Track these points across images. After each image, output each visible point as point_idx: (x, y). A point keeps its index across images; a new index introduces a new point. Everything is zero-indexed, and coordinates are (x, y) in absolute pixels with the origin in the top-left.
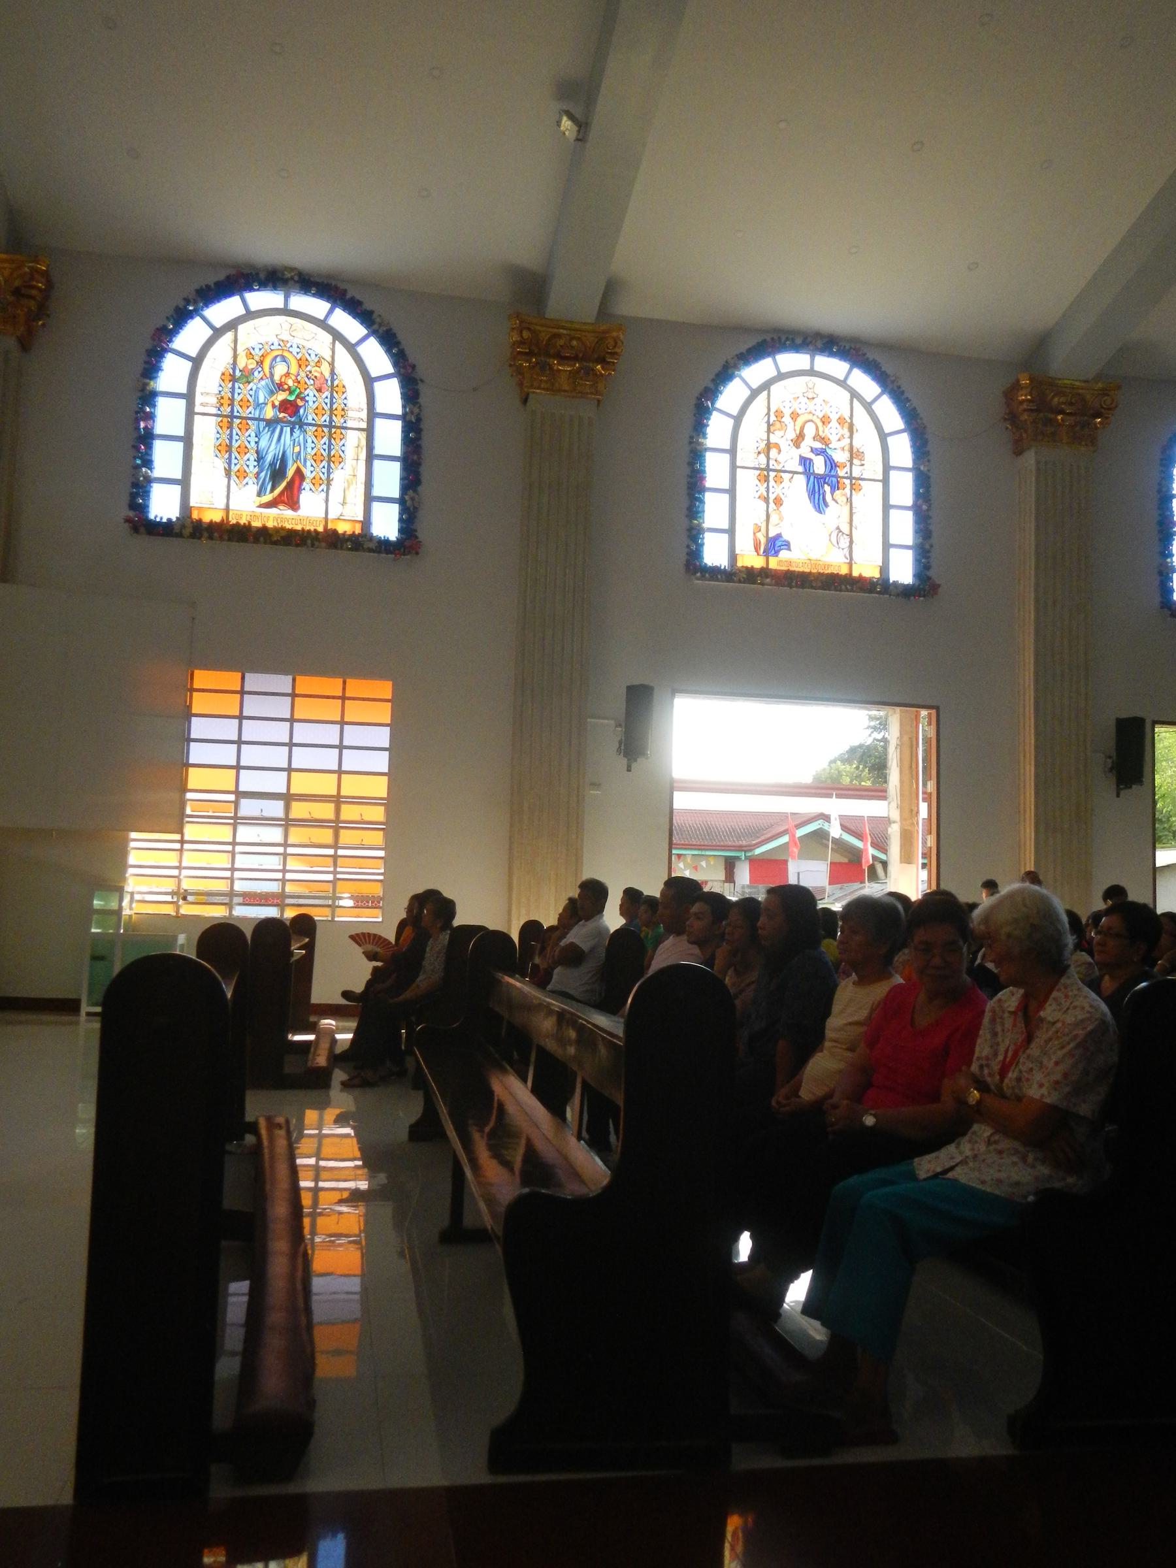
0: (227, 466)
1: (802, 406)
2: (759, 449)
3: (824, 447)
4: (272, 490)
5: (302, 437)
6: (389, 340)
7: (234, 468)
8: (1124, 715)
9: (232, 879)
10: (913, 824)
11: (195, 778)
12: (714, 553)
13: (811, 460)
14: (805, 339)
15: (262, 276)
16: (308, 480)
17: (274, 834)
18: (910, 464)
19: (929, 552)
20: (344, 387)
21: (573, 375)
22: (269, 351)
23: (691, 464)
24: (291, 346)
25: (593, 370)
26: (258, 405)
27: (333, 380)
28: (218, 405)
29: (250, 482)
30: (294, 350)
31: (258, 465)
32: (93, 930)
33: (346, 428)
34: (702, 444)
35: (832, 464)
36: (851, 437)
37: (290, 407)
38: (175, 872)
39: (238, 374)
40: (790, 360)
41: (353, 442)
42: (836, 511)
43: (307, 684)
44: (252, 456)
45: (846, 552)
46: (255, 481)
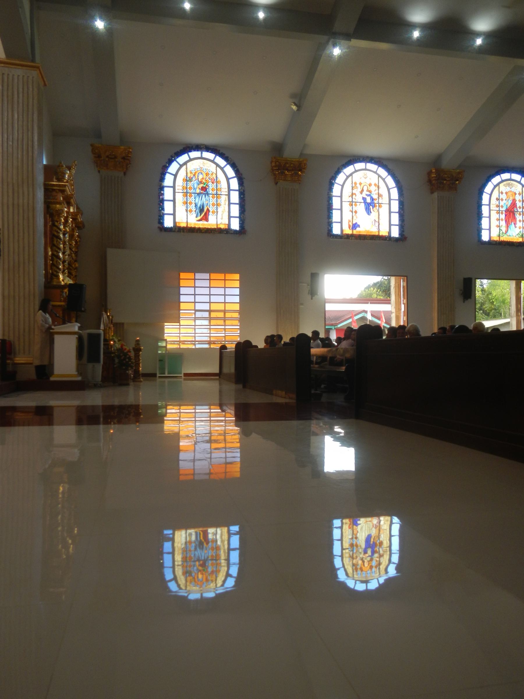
0: (186, 209)
1: (363, 181)
2: (350, 195)
3: (370, 193)
4: (200, 216)
5: (208, 198)
6: (234, 166)
7: (189, 209)
8: (466, 276)
9: (195, 337)
10: (400, 313)
11: (182, 306)
12: (336, 230)
13: (366, 198)
14: (363, 158)
15: (194, 147)
17: (206, 322)
18: (397, 198)
19: (404, 226)
20: (220, 181)
21: (292, 175)
22: (197, 171)
23: (328, 202)
25: (297, 173)
26: (194, 189)
30: (205, 170)
32: (159, 352)
33: (221, 195)
34: (331, 195)
35: (372, 199)
36: (378, 190)
37: (204, 189)
38: (178, 335)
39: (188, 179)
40: (360, 166)
41: (223, 199)
42: (374, 214)
43: (214, 276)
44: (194, 205)
45: (377, 227)
46: (195, 213)
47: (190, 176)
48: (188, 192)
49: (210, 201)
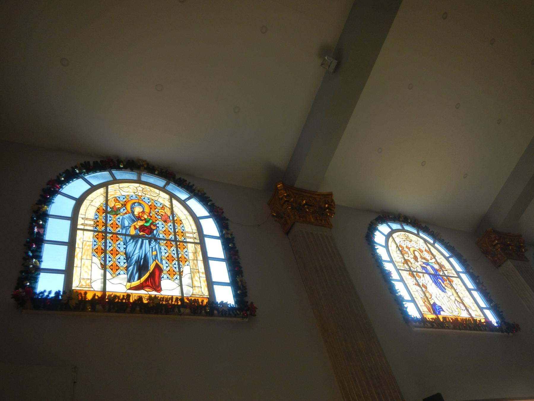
4: (139, 278)
5: (157, 246)
6: (204, 200)
7: (109, 264)
16: (165, 272)
20: (181, 221)
24: (144, 198)
26: (123, 227)
29: (122, 272)
31: (127, 262)
36: (435, 258)
39: (109, 209)
47: (115, 206)
48: (108, 231)
49: (162, 251)
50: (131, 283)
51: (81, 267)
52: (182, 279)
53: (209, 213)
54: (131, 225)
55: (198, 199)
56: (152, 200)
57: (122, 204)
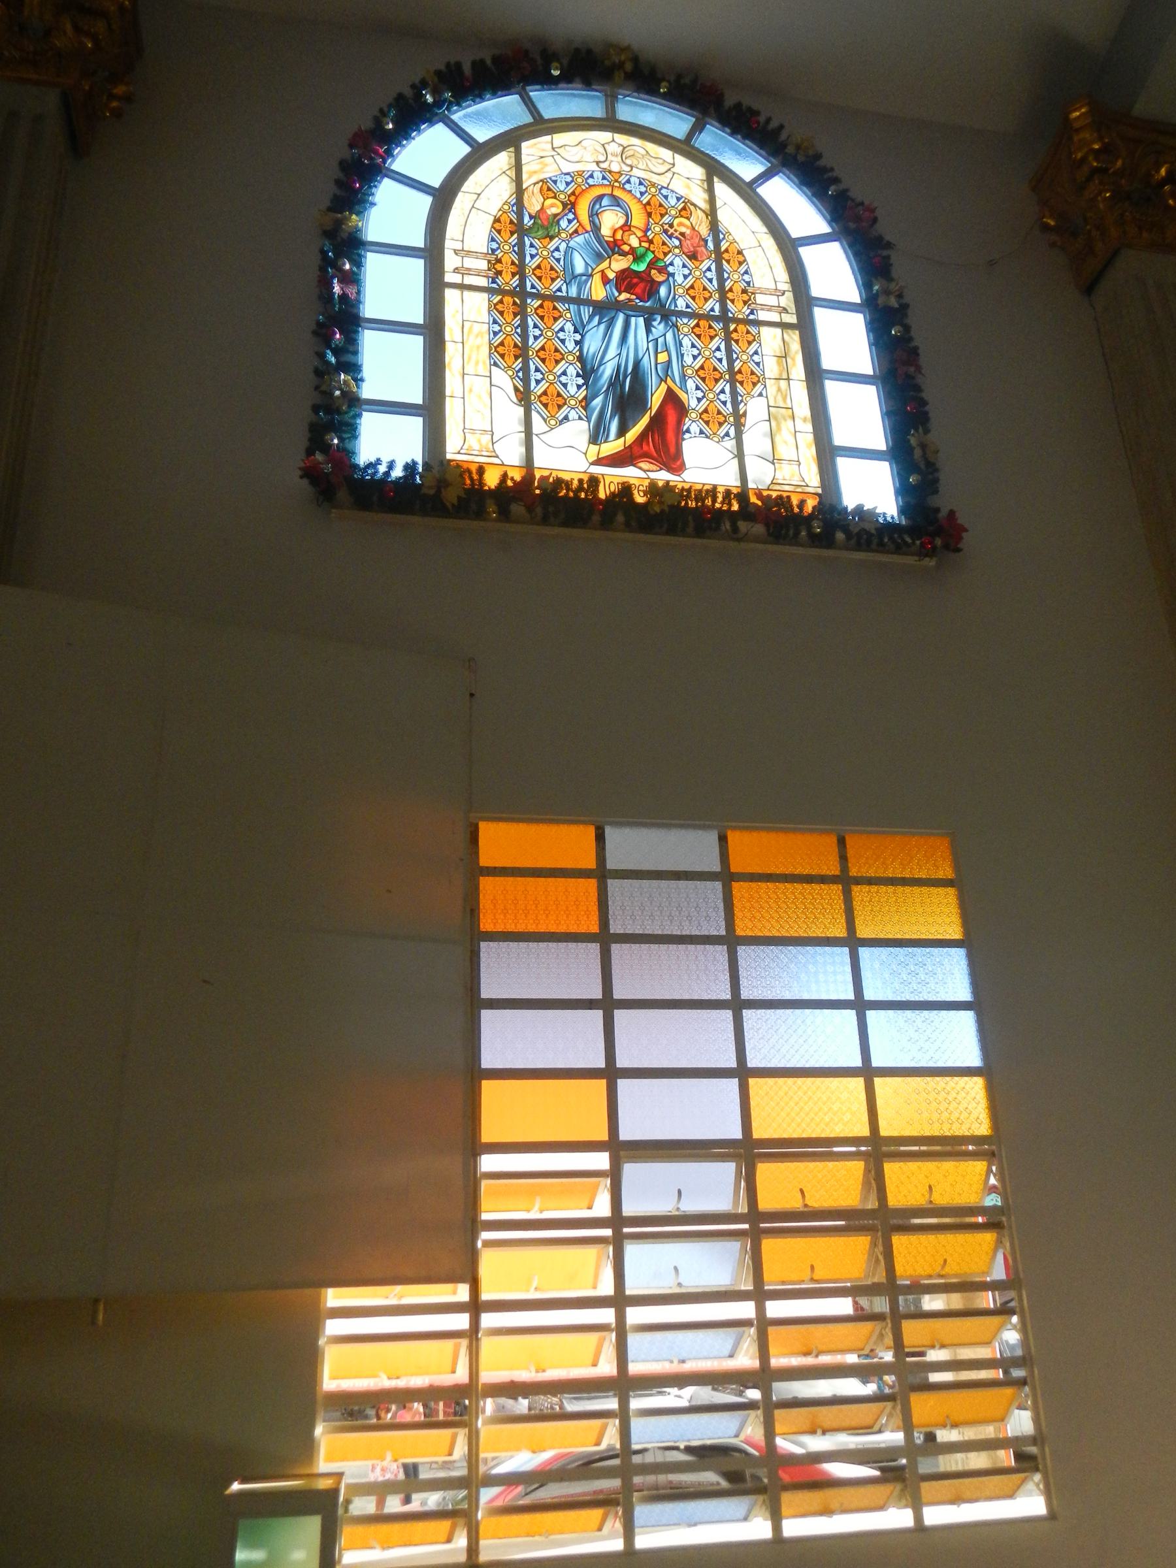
4: (622, 432)
5: (669, 336)
9: (623, 1415)
16: (694, 415)
20: (740, 253)
24: (628, 181)
27: (717, 243)
28: (491, 274)
29: (573, 415)
31: (586, 383)
47: (542, 208)
49: (684, 350)
50: (600, 445)
51: (464, 398)
52: (743, 435)
53: (829, 223)
54: (593, 270)
55: (795, 175)
56: (653, 185)
57: (562, 202)
